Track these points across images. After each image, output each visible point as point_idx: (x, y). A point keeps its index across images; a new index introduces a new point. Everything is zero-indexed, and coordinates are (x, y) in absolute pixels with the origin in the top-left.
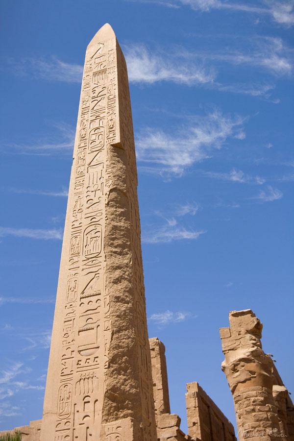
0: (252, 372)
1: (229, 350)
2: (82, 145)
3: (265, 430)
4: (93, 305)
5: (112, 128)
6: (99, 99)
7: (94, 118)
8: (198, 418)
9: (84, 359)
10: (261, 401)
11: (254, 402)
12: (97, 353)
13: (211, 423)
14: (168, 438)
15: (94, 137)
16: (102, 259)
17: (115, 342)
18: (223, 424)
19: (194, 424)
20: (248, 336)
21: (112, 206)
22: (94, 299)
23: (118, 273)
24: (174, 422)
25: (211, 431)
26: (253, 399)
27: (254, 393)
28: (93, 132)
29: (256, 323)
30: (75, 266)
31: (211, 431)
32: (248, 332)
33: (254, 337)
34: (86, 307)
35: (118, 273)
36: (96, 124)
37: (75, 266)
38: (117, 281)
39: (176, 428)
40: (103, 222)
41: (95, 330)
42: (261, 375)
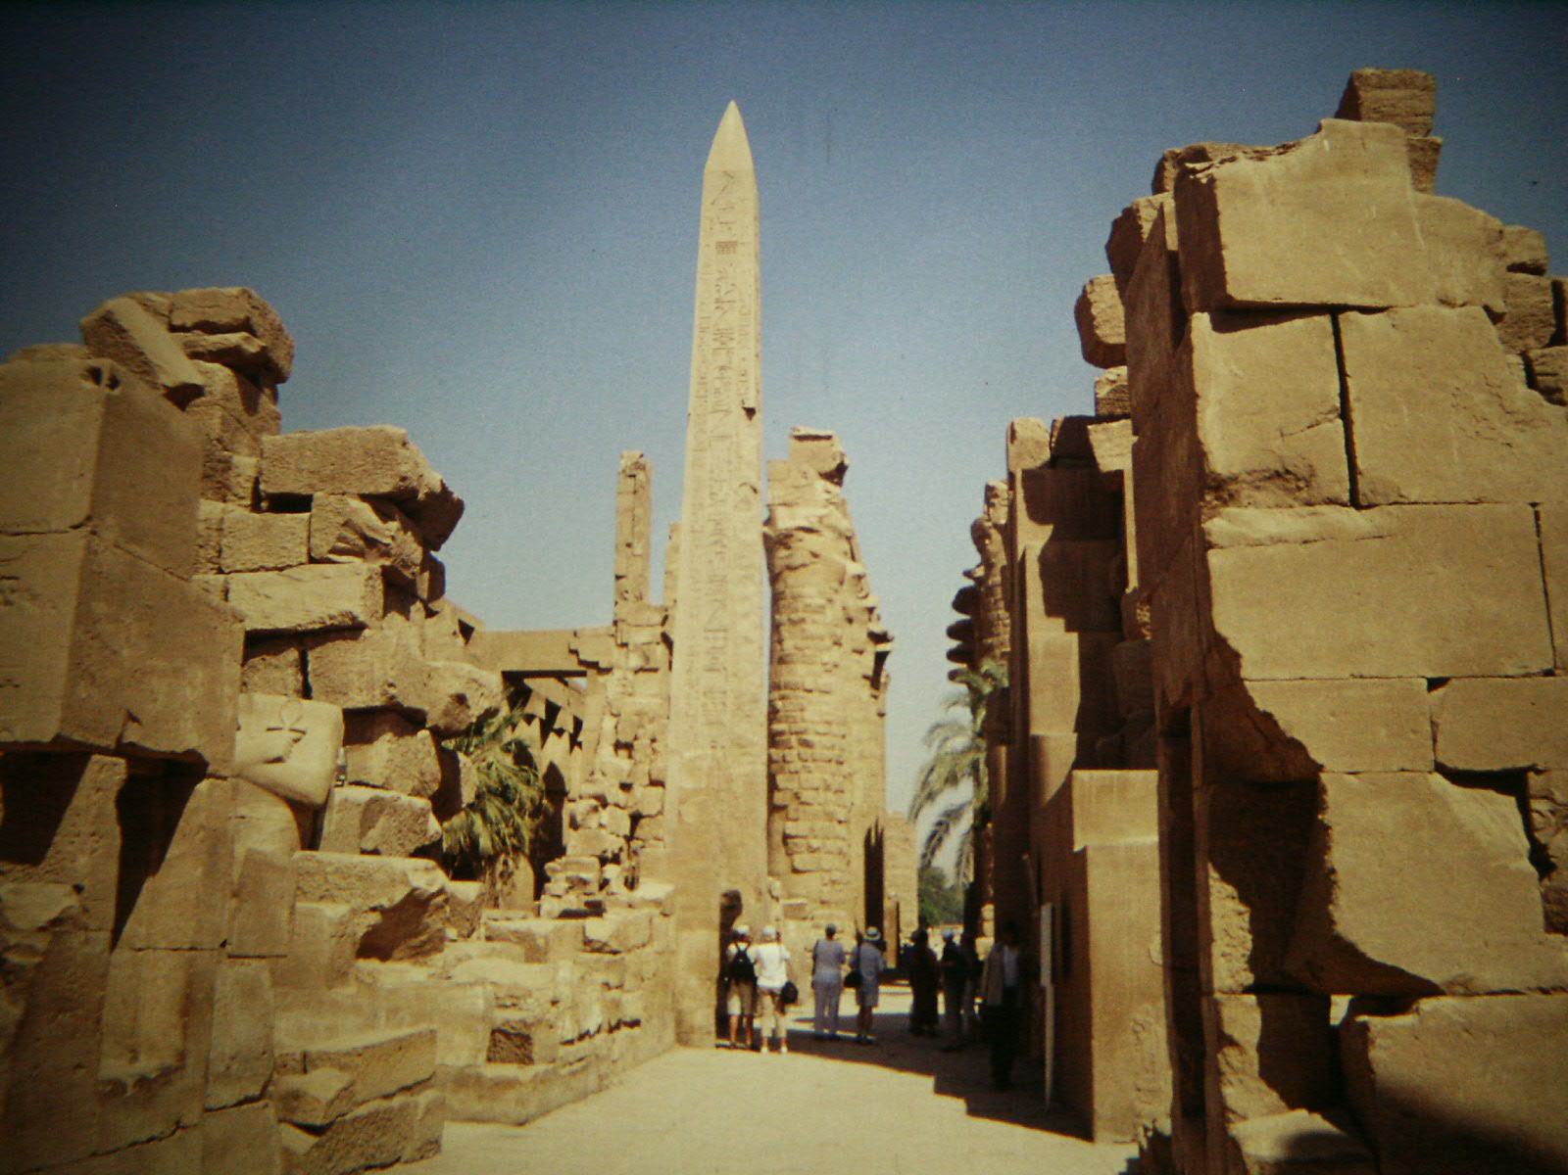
1: (780, 505)
2: (702, 393)
4: (720, 643)
5: (743, 375)
6: (726, 306)
7: (717, 344)
14: (644, 644)
15: (718, 384)
20: (822, 484)
22: (721, 634)
24: (658, 618)
28: (716, 373)
29: (838, 462)
36: (722, 359)
39: (659, 630)
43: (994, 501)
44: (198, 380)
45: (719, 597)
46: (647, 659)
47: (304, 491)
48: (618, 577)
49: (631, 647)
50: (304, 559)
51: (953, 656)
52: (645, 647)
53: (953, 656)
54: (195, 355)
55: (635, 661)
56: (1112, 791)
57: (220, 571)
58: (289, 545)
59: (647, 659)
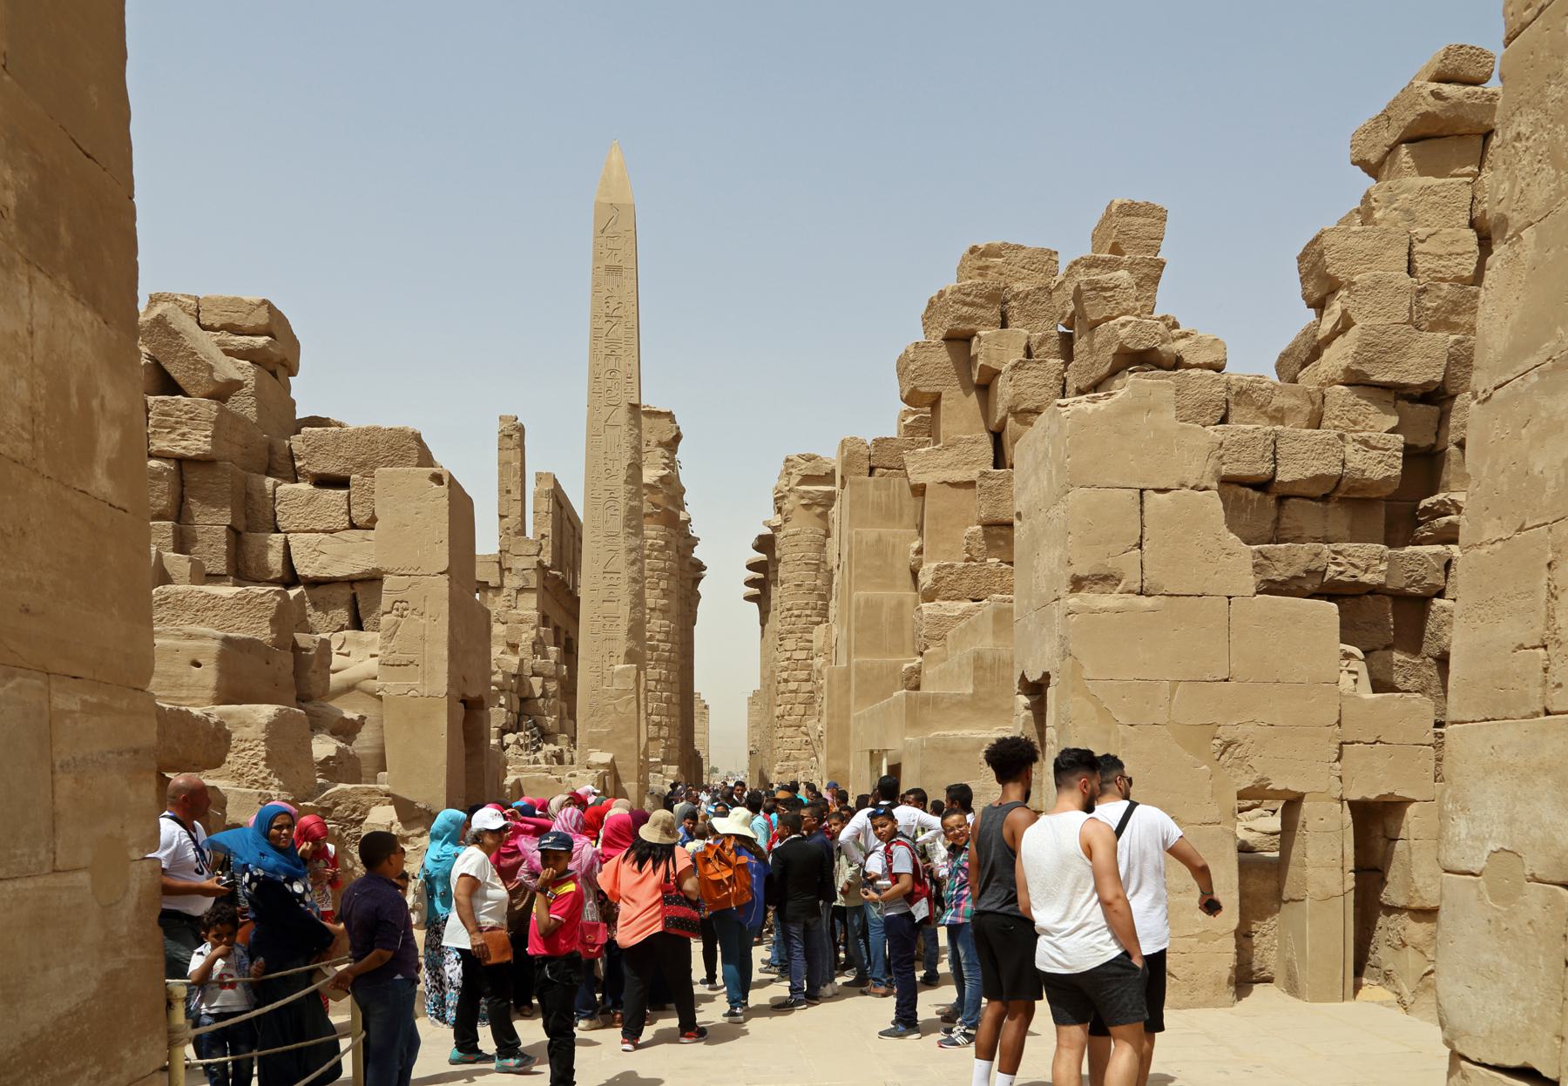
0: (655, 505)
3: (658, 583)
8: (550, 529)
9: (608, 624)
10: (661, 547)
11: (651, 545)
12: (618, 622)
13: (562, 532)
16: (622, 540)
17: (632, 615)
18: (574, 528)
19: (543, 536)
20: (660, 451)
21: (629, 484)
23: (633, 555)
24: (534, 550)
25: (561, 543)
26: (650, 541)
27: (653, 534)
29: (674, 434)
30: (596, 539)
31: (561, 543)
32: (660, 444)
33: (667, 454)
34: (607, 582)
35: (633, 555)
37: (596, 539)
38: (633, 563)
39: (536, 559)
40: (622, 500)
41: (615, 604)
42: (666, 510)
43: (793, 471)
44: (238, 376)
45: (616, 548)
46: (527, 581)
47: (342, 474)
48: (501, 517)
49: (513, 571)
50: (346, 524)
51: (749, 583)
52: (525, 572)
53: (750, 583)
54: (228, 353)
55: (517, 582)
56: (929, 704)
57: (279, 532)
58: (333, 514)
59: (527, 581)
